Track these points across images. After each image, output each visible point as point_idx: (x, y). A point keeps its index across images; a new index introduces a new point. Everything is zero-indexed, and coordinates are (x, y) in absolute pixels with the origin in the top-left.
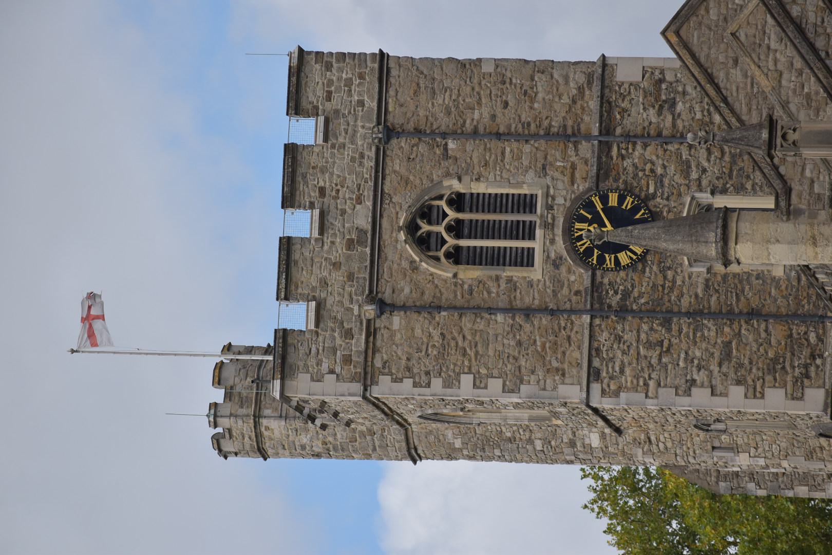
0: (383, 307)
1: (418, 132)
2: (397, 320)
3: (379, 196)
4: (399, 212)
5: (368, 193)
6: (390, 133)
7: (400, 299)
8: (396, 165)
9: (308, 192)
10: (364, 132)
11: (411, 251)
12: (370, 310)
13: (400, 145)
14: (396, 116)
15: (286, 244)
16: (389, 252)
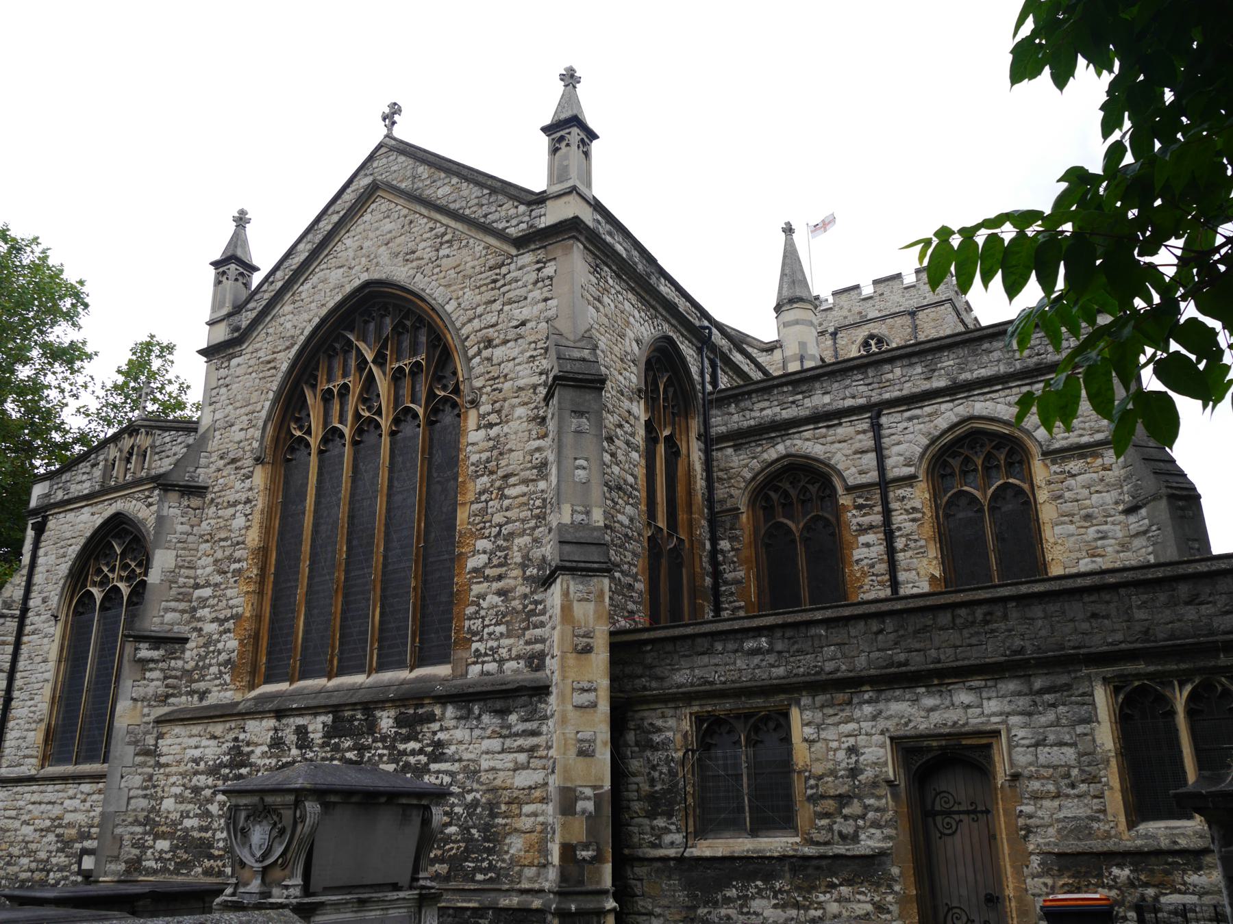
0: (834, 334)
1: (916, 326)
2: (830, 342)
3: (883, 318)
4: (876, 329)
5: (883, 313)
6: (912, 314)
7: (839, 341)
8: (899, 321)
9: (881, 288)
10: (911, 303)
11: (860, 339)
12: (831, 330)
13: (907, 320)
14: (921, 315)
15: (857, 287)
16: (860, 330)
